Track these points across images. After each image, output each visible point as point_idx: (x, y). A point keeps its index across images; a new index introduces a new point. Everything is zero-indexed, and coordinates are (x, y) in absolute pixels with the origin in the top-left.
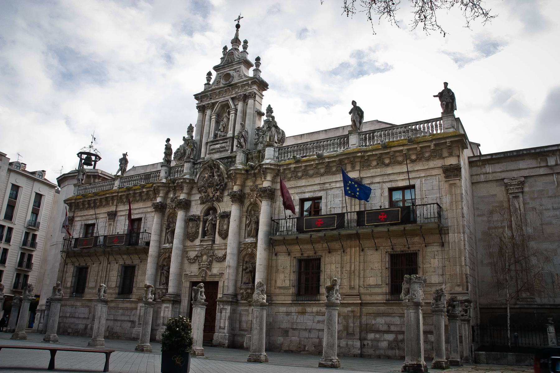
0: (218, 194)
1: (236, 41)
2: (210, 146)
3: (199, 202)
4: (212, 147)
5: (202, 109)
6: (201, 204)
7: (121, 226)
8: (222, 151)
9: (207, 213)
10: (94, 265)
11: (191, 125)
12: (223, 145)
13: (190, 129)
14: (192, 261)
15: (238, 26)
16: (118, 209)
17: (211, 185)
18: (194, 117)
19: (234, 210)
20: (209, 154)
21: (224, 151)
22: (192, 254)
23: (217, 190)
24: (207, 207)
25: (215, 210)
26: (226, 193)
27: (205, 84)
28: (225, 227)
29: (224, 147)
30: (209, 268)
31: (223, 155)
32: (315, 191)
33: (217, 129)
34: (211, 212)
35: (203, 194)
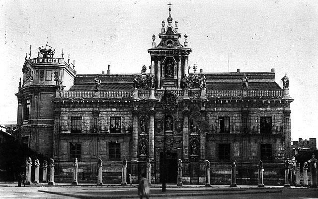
1: (170, 20)
5: (153, 59)
9: (166, 117)
13: (144, 68)
15: (170, 10)
19: (186, 120)
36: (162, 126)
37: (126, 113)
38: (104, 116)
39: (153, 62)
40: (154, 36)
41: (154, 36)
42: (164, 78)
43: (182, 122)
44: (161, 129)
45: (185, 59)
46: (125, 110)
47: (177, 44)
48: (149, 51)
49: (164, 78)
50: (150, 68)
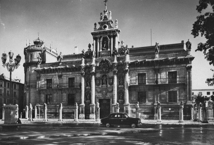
5: (95, 39)
7: (65, 80)
9: (103, 76)
10: (55, 94)
11: (90, 44)
13: (90, 46)
14: (98, 93)
16: (63, 74)
18: (92, 41)
19: (116, 78)
22: (99, 90)
25: (106, 76)
27: (94, 28)
28: (111, 82)
30: (106, 94)
32: (143, 71)
33: (103, 46)
34: (105, 76)
35: (101, 70)
36: (100, 82)
37: (77, 75)
38: (65, 77)
39: (95, 41)
40: (95, 24)
41: (95, 24)
42: (102, 51)
43: (113, 78)
44: (99, 85)
45: (114, 37)
46: (77, 73)
47: (110, 27)
48: (92, 34)
49: (102, 51)
50: (93, 45)
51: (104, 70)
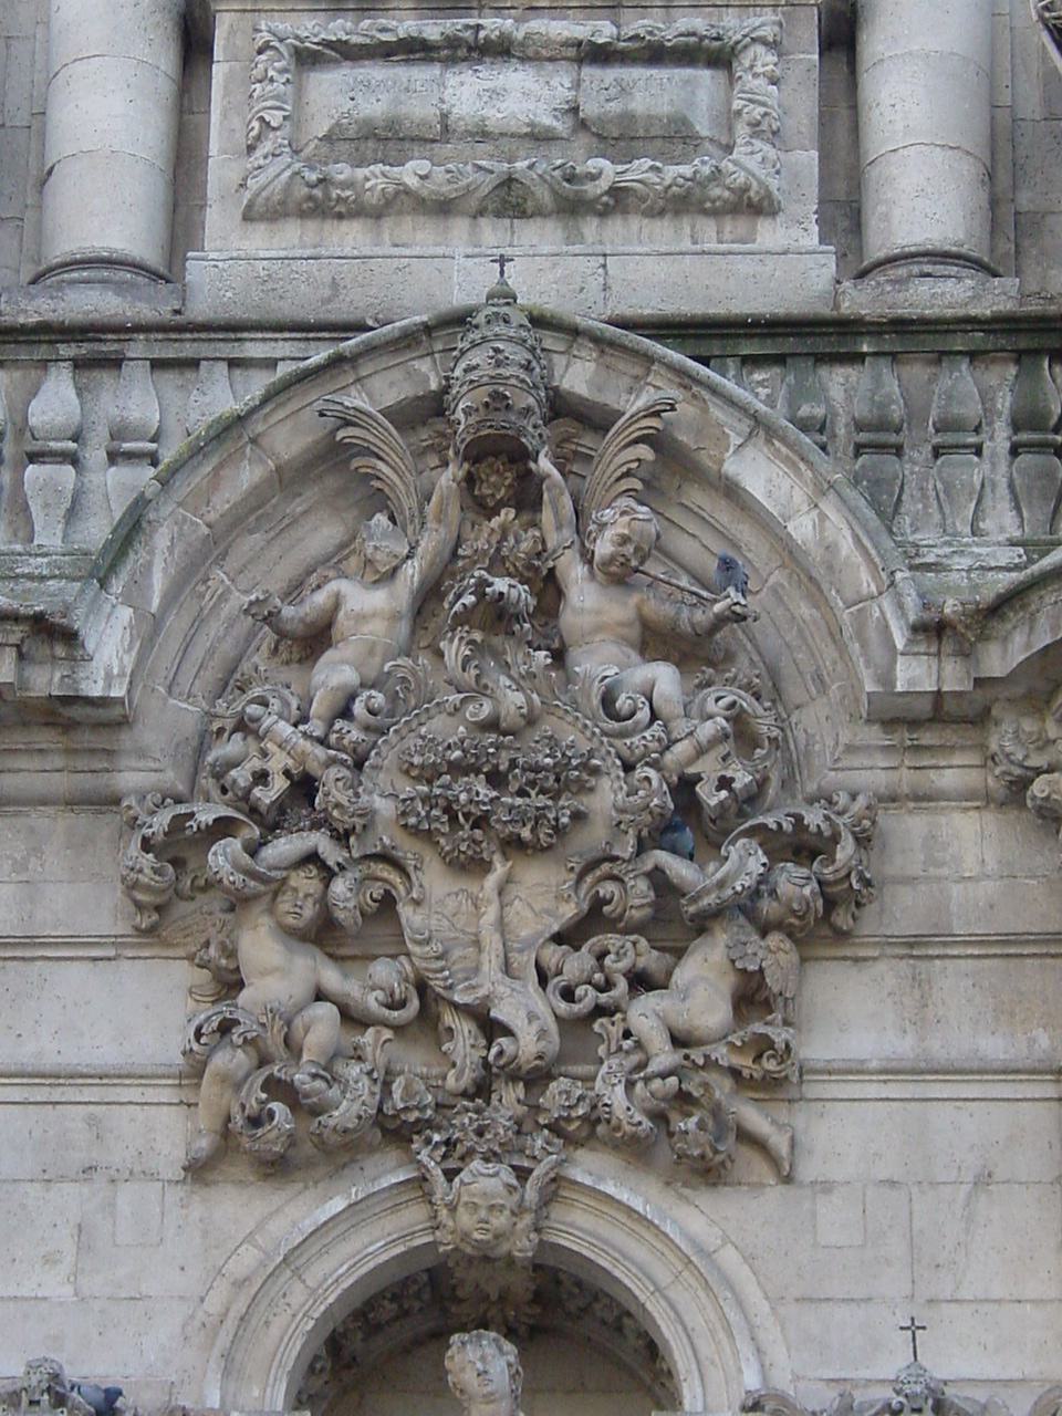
0: (700, 990)
2: (307, 58)
3: (167, 1132)
4: (338, 95)
6: (199, 1171)
8: (619, 201)
12: (653, 92)
17: (495, 806)
20: (321, 206)
21: (681, 203)
23: (675, 923)
24: (371, 1248)
26: (851, 1015)
29: (677, 136)
31: (658, 269)
35: (276, 971)
51: (491, 929)
